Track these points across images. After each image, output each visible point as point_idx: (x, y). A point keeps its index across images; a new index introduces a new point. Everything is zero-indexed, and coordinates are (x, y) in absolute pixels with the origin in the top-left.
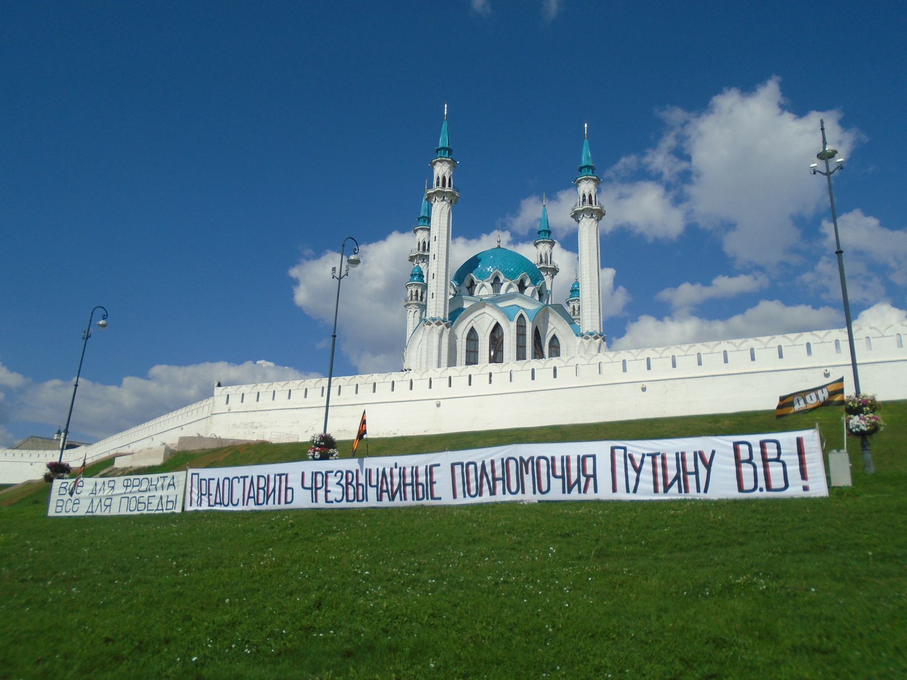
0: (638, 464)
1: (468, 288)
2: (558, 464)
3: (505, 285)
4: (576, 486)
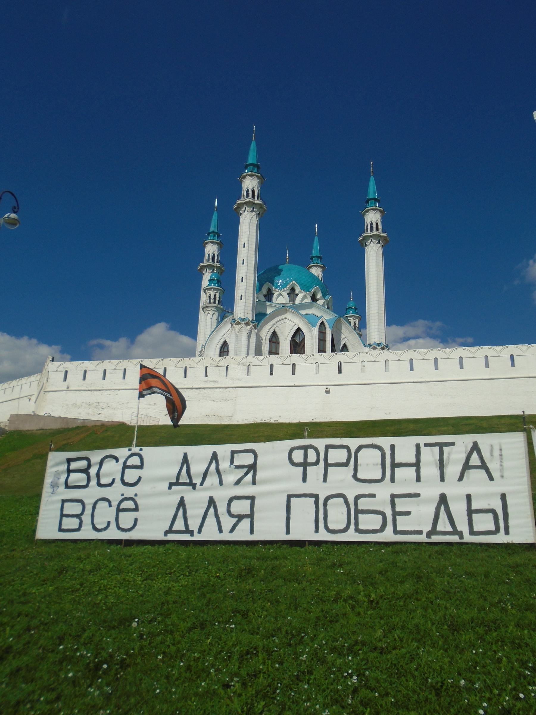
1: (265, 296)
3: (300, 296)
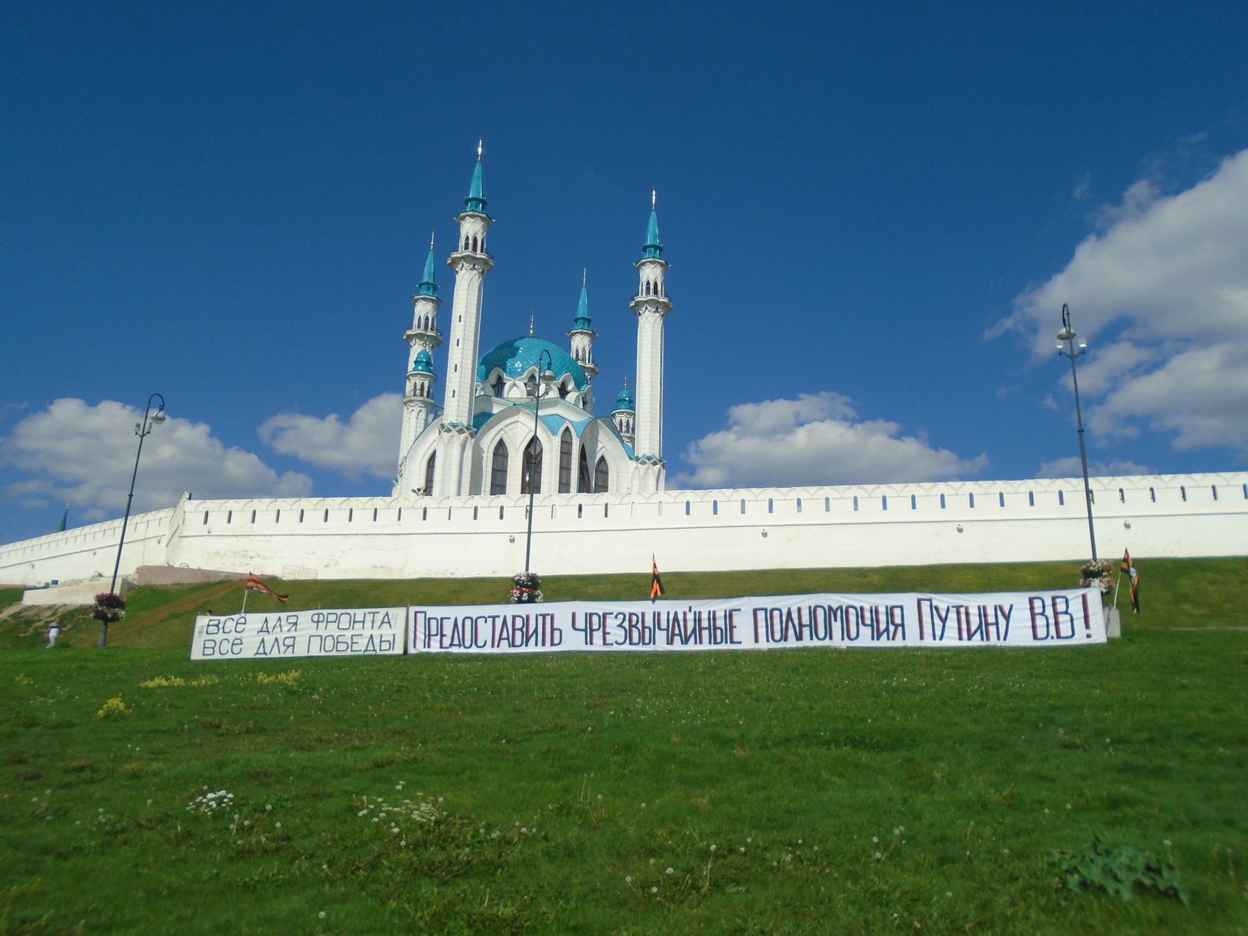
0: (943, 614)
1: (493, 386)
2: (867, 615)
4: (885, 635)
